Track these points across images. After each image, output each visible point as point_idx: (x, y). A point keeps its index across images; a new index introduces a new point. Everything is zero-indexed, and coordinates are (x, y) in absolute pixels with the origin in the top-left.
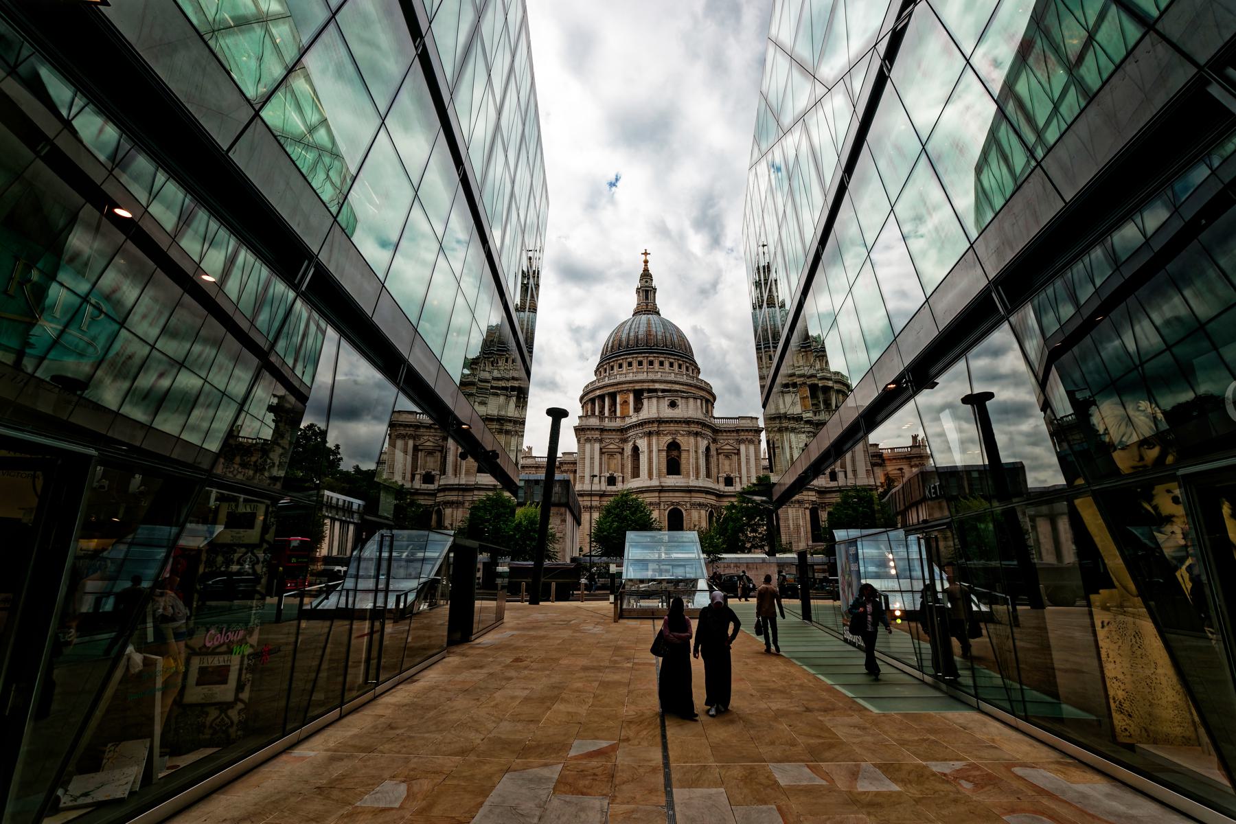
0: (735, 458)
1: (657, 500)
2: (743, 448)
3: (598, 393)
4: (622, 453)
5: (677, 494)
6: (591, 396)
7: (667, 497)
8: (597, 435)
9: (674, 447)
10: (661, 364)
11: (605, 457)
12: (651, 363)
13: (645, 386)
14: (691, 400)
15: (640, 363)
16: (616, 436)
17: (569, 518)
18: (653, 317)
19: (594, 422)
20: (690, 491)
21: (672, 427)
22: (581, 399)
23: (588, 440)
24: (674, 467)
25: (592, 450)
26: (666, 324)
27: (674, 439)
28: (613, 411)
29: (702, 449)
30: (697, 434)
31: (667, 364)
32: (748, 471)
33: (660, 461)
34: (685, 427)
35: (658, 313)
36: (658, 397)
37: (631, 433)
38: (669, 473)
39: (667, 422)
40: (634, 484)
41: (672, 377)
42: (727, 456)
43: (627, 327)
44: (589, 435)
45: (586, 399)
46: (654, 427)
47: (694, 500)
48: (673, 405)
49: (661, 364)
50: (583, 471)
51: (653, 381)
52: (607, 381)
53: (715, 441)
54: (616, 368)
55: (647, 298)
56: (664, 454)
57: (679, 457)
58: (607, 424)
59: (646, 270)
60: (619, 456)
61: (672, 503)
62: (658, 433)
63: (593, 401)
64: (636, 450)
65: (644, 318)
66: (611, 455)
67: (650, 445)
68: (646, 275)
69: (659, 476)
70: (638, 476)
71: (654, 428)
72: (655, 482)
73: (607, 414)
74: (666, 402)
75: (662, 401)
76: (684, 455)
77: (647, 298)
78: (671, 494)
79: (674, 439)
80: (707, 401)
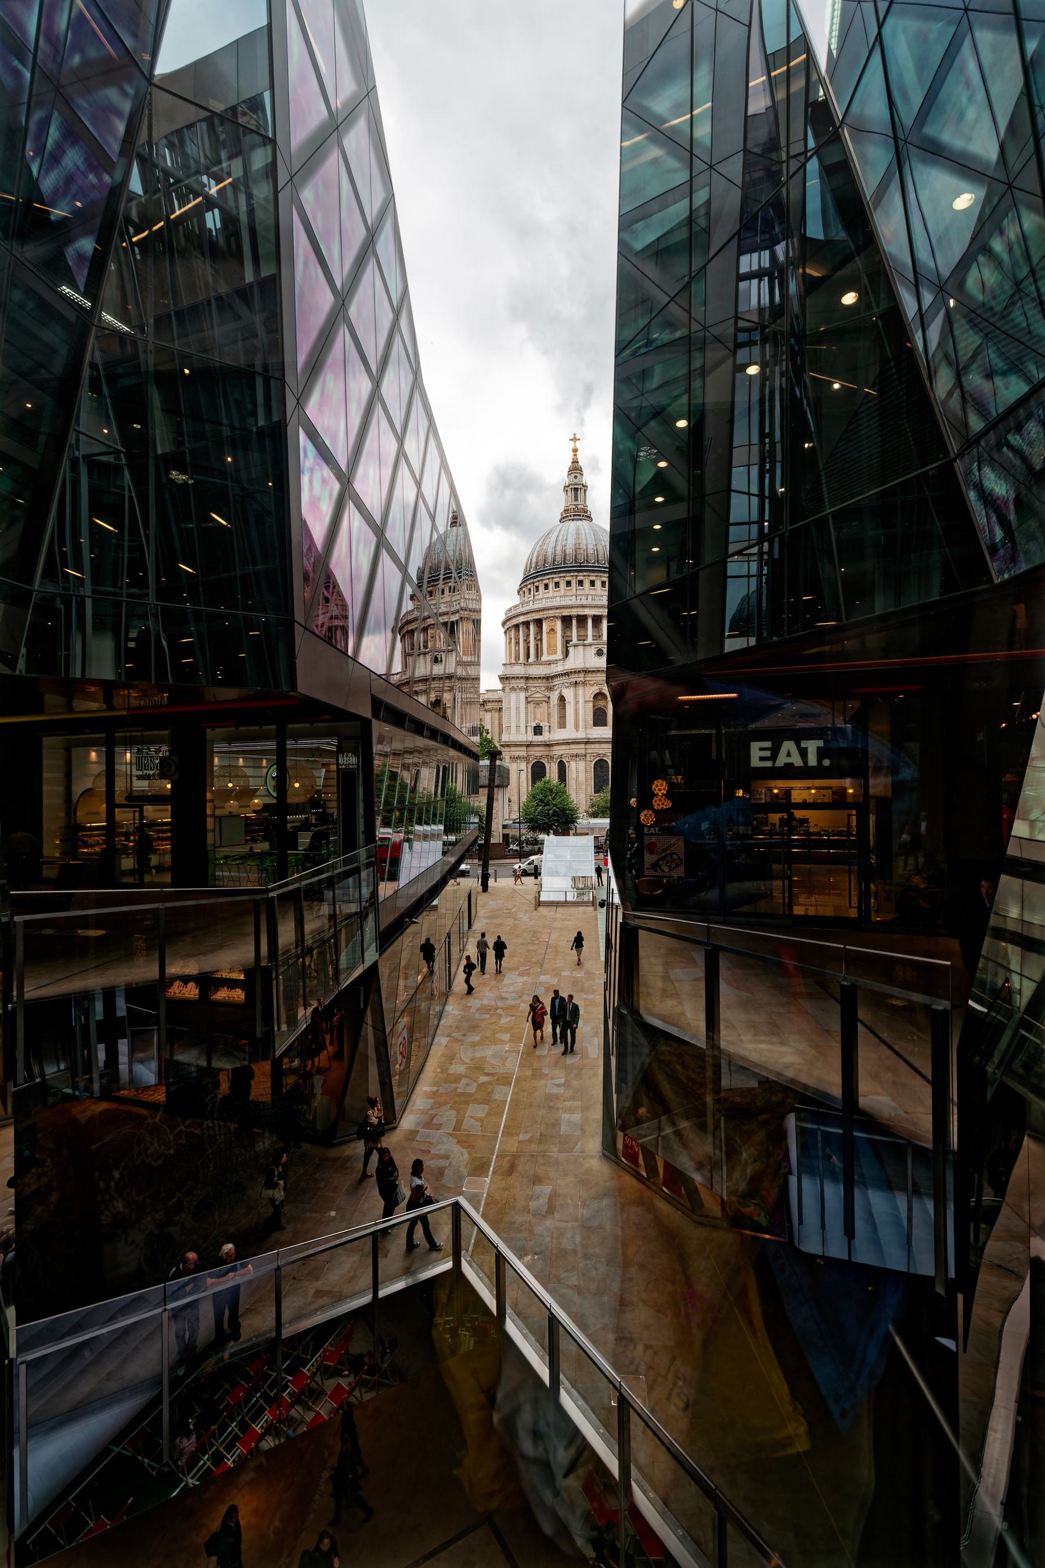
1: (583, 752)
3: (522, 619)
6: (514, 622)
8: (522, 683)
11: (531, 706)
12: (581, 583)
13: (574, 612)
15: (569, 583)
16: (542, 684)
18: (584, 524)
19: (519, 670)
23: (513, 689)
25: (518, 700)
28: (539, 640)
35: (589, 518)
37: (557, 681)
38: (596, 724)
40: (559, 735)
43: (553, 539)
44: (514, 683)
45: (509, 624)
49: (592, 583)
50: (509, 721)
51: (583, 606)
52: (531, 606)
55: (576, 499)
56: (591, 705)
59: (575, 462)
60: (545, 705)
62: (584, 683)
63: (517, 626)
64: (562, 699)
66: (537, 703)
67: (576, 696)
70: (565, 727)
72: (581, 735)
77: (576, 499)
78: (597, 746)
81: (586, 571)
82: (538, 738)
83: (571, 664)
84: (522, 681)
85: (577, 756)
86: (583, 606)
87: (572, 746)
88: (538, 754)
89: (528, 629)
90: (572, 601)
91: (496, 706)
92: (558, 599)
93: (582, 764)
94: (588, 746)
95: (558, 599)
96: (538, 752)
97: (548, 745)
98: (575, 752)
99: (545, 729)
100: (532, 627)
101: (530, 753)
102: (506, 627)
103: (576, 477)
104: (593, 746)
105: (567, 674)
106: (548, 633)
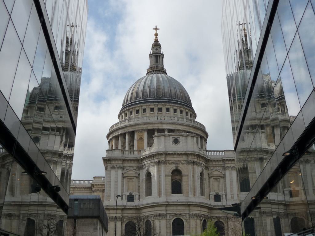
0: (222, 180)
1: (164, 212)
2: (227, 173)
3: (120, 132)
4: (138, 177)
5: (179, 208)
6: (116, 134)
7: (172, 210)
8: (120, 164)
9: (177, 172)
10: (168, 110)
11: (126, 180)
12: (160, 109)
13: (156, 127)
14: (189, 138)
15: (152, 110)
16: (135, 165)
17: (99, 227)
19: (117, 154)
20: (189, 205)
21: (176, 158)
22: (108, 136)
23: (113, 168)
24: (177, 188)
26: (171, 81)
27: (177, 167)
28: (132, 146)
29: (198, 175)
30: (194, 163)
31: (172, 110)
32: (232, 190)
33: (167, 183)
34: (185, 158)
36: (165, 136)
37: (146, 162)
39: (172, 154)
40: (147, 200)
41: (175, 120)
42: (216, 179)
44: (114, 164)
46: (161, 158)
47: (191, 212)
48: (176, 141)
49: (168, 110)
51: (162, 123)
52: (127, 123)
53: (207, 168)
54: (134, 113)
55: (157, 61)
56: (170, 178)
57: (181, 180)
58: (128, 156)
61: (176, 214)
62: (165, 162)
64: (149, 175)
65: (155, 75)
66: (130, 178)
67: (159, 172)
68: (156, 45)
69: (166, 194)
71: (162, 158)
72: (163, 199)
73: (127, 148)
74: (171, 139)
75: (168, 138)
76: (184, 179)
77: (157, 61)
78: (175, 208)
79: (177, 167)
80: (202, 138)
81: (163, 102)
82: (132, 204)
83: (155, 149)
84: (120, 162)
85: (160, 215)
86: (162, 123)
87: (156, 209)
88: (130, 216)
89: (125, 139)
90: (154, 119)
91: (100, 188)
92: (145, 118)
93: (163, 222)
94: (168, 208)
95: (145, 118)
96: (129, 214)
97: (138, 209)
98: (158, 213)
99: (137, 197)
100: (127, 137)
101: (125, 215)
102: (110, 138)
103: (157, 49)
104: (172, 208)
105: (153, 156)
106: (138, 140)
